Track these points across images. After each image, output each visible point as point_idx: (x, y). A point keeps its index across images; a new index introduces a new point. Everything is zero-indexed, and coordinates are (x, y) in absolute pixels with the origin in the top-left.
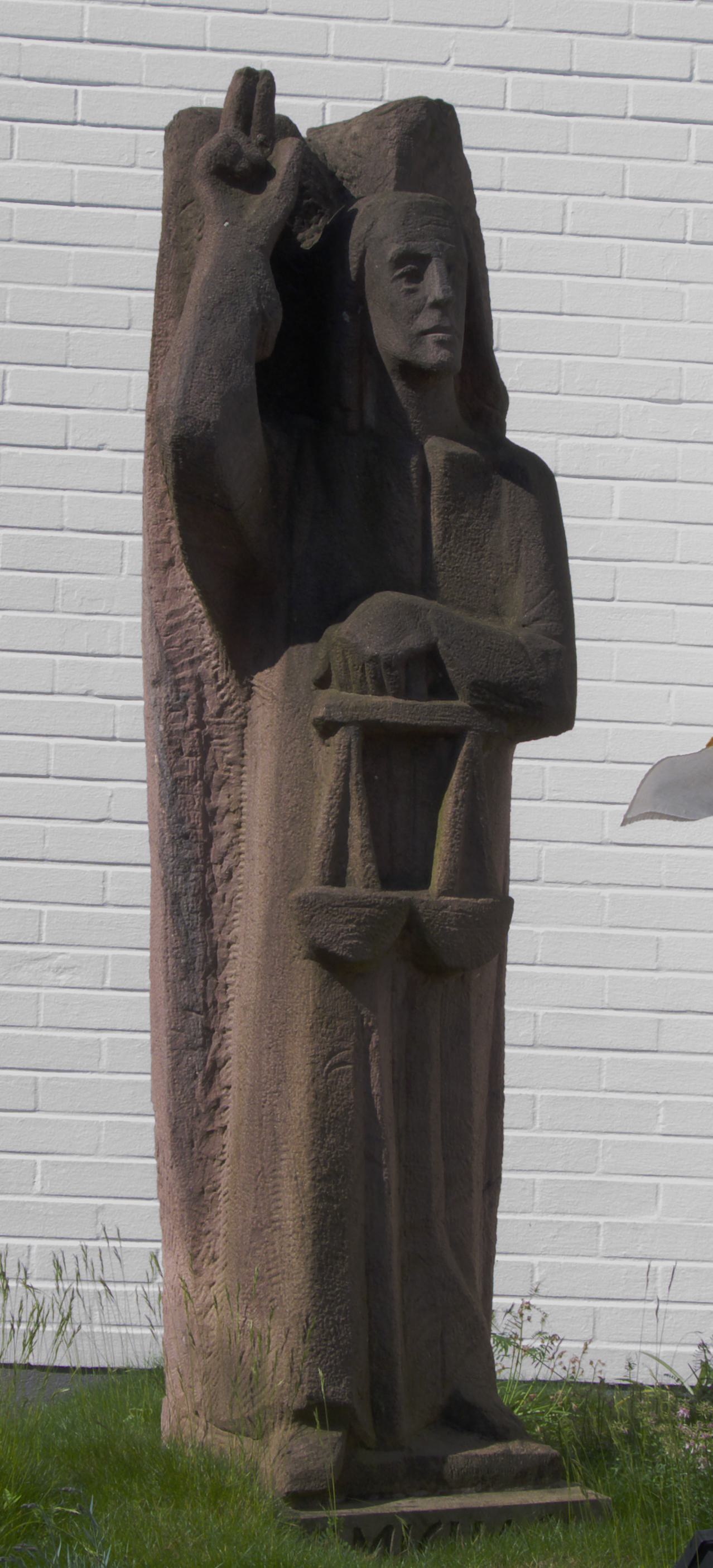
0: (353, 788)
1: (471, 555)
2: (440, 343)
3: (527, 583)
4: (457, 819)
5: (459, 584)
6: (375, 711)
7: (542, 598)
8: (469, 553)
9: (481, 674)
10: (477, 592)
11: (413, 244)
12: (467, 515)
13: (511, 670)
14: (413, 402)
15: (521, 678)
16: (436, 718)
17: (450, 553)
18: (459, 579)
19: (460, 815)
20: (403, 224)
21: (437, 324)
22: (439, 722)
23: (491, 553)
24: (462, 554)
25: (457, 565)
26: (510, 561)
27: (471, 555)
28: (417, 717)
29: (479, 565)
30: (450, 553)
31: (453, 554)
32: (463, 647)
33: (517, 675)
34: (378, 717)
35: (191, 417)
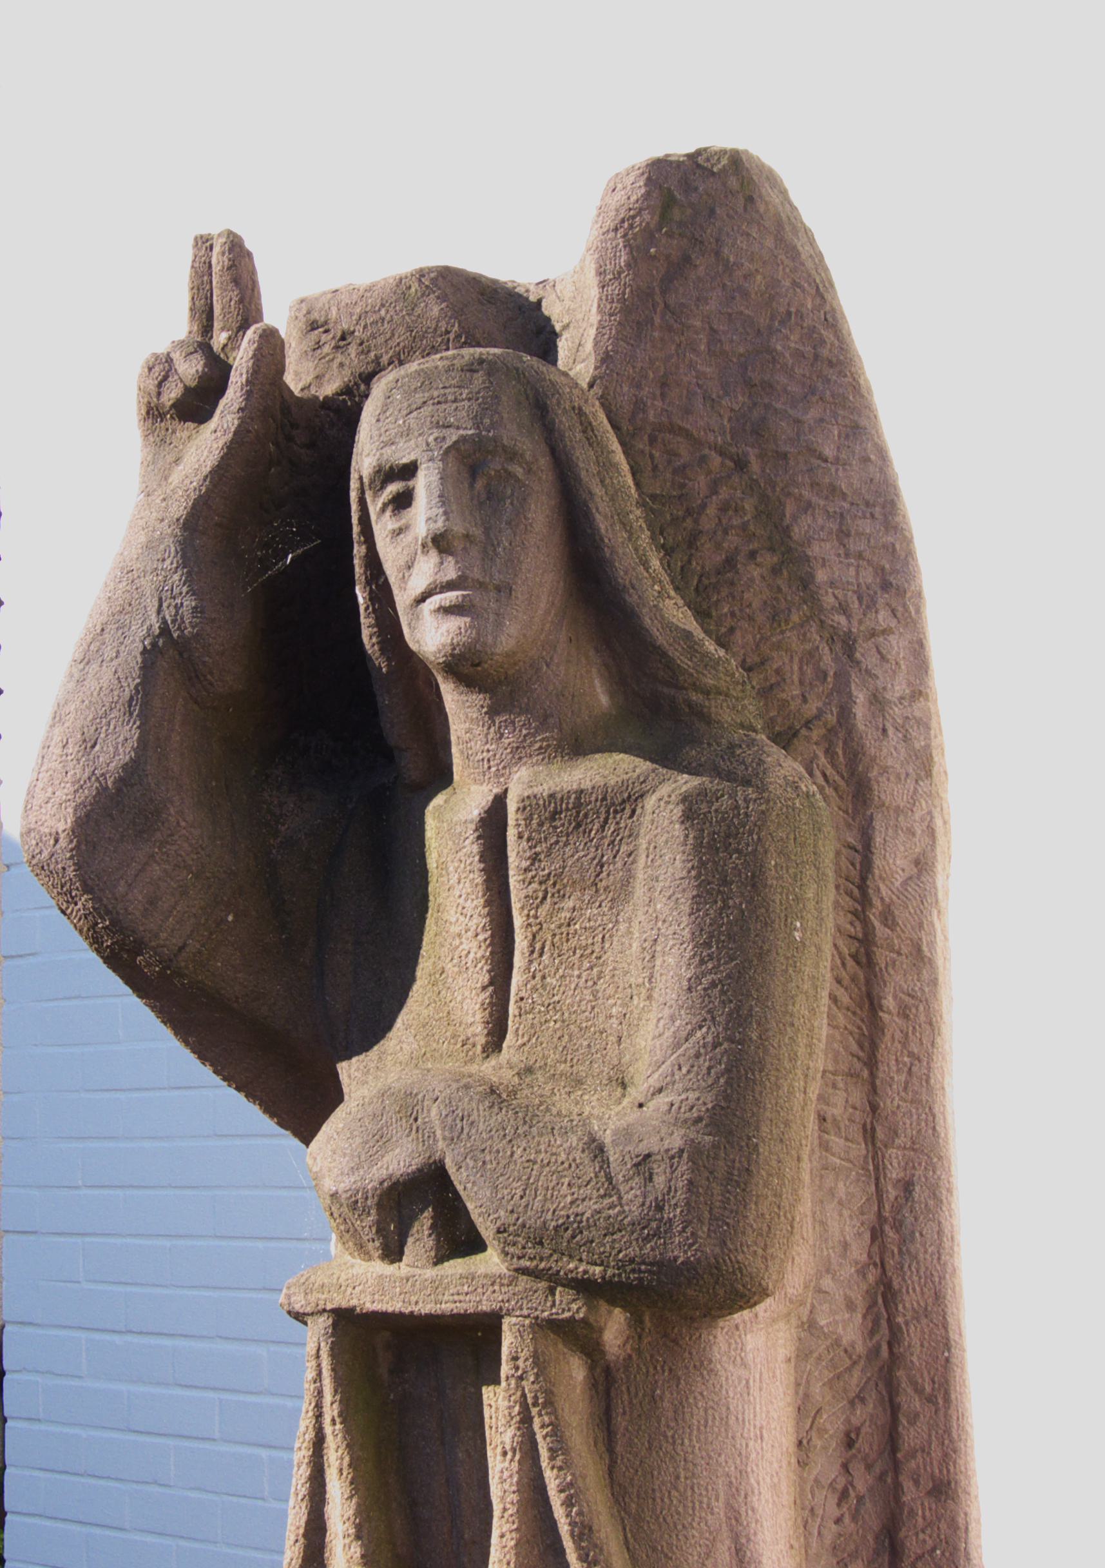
0: (328, 1429)
1: (579, 977)
2: (447, 610)
3: (659, 1020)
4: (506, 1486)
5: (559, 1034)
6: (349, 1290)
7: (677, 1046)
8: (576, 973)
9: (512, 1211)
10: (589, 1046)
11: (388, 451)
12: (570, 904)
13: (569, 1199)
14: (475, 716)
15: (587, 1215)
16: (446, 1298)
17: (544, 977)
18: (558, 1025)
19: (511, 1476)
20: (378, 420)
21: (431, 580)
22: (453, 1306)
23: (615, 969)
24: (563, 976)
25: (556, 998)
26: (640, 980)
27: (579, 977)
28: (414, 1299)
29: (595, 994)
30: (544, 977)
31: (548, 980)
32: (484, 1163)
33: (580, 1209)
34: (354, 1302)
35: (34, 829)
